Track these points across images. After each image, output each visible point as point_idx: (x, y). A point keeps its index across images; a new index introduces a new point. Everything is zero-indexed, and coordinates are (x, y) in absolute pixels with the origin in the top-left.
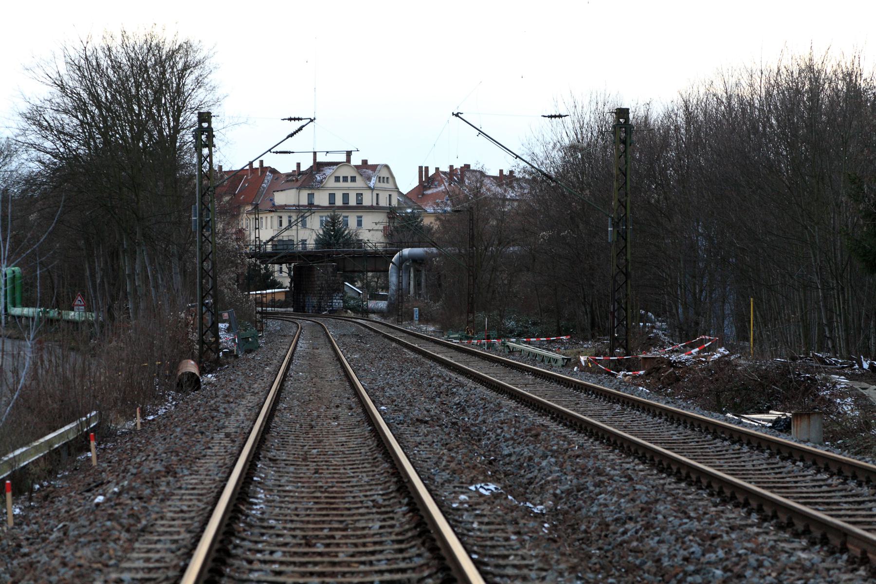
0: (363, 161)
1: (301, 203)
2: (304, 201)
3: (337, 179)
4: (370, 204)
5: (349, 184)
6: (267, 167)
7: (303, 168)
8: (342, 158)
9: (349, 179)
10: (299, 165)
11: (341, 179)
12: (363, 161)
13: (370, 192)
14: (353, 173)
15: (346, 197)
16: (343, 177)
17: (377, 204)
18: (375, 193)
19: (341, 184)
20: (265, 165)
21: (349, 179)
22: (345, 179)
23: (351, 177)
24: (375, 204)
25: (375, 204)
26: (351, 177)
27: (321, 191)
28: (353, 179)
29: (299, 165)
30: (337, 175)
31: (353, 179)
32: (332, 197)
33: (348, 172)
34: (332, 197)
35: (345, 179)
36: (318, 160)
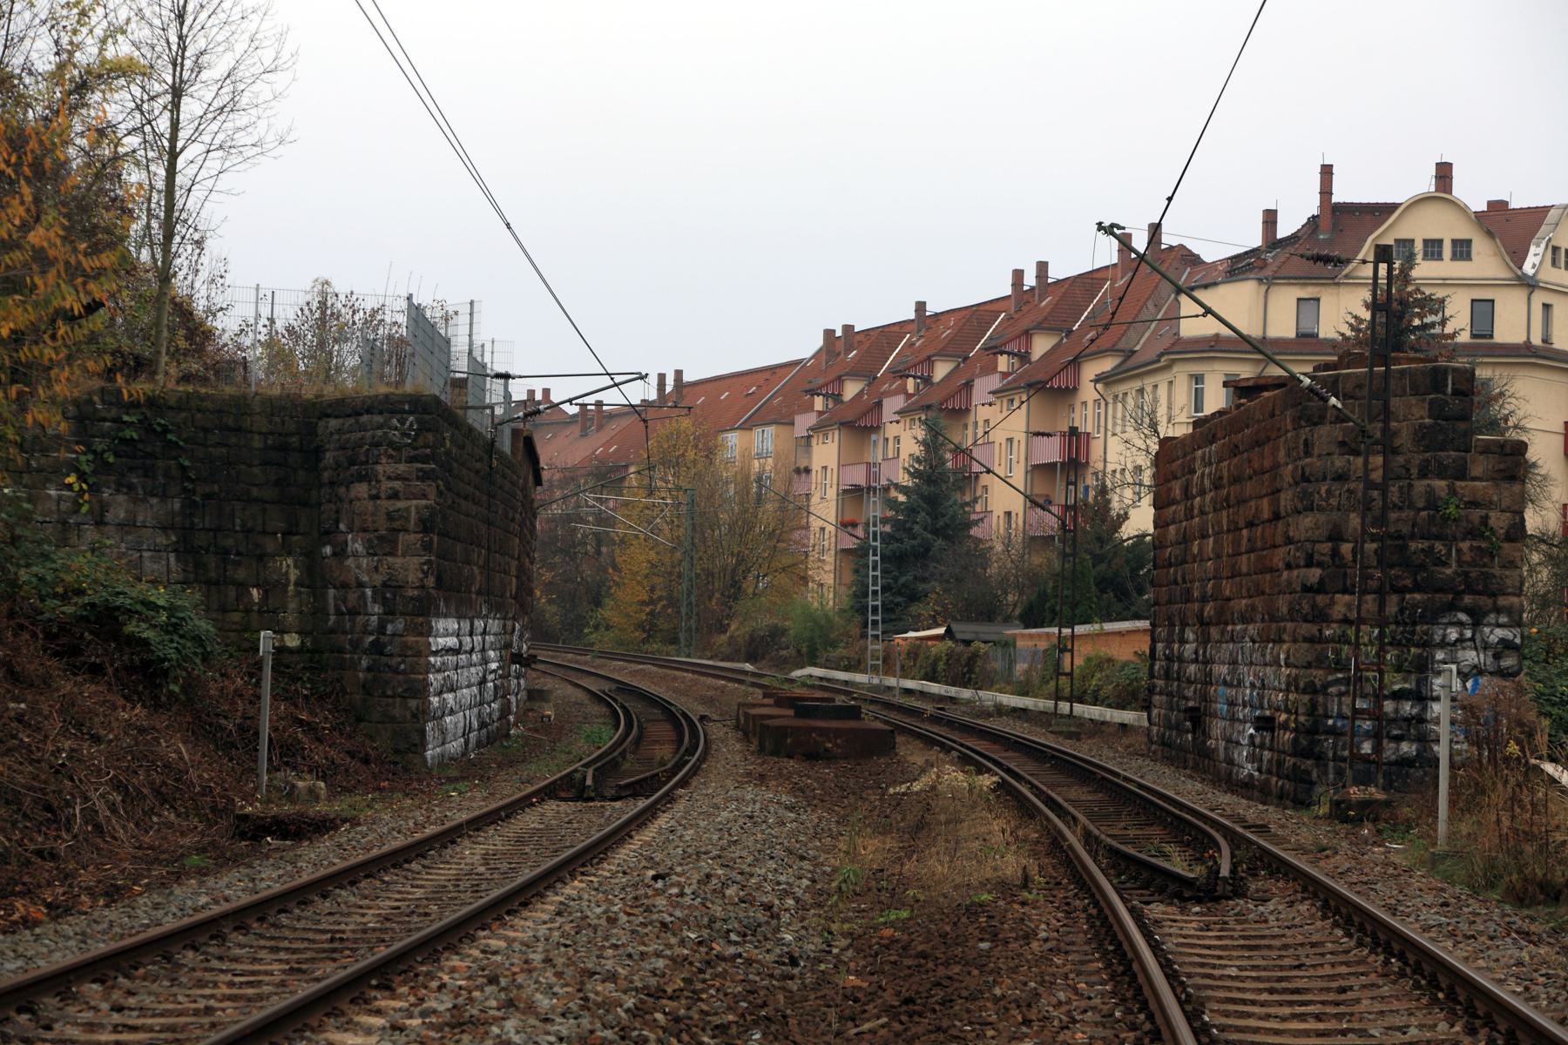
0: (1490, 204)
1: (1273, 333)
4: (1518, 338)
5: (1447, 267)
6: (1171, 248)
7: (1283, 231)
10: (1270, 218)
12: (1490, 204)
13: (1519, 296)
14: (1463, 231)
17: (1544, 341)
18: (1539, 298)
23: (1455, 242)
24: (1536, 340)
25: (1536, 340)
26: (1455, 242)
27: (1342, 290)
28: (1462, 250)
29: (1270, 218)
33: (1445, 227)
36: (1338, 197)
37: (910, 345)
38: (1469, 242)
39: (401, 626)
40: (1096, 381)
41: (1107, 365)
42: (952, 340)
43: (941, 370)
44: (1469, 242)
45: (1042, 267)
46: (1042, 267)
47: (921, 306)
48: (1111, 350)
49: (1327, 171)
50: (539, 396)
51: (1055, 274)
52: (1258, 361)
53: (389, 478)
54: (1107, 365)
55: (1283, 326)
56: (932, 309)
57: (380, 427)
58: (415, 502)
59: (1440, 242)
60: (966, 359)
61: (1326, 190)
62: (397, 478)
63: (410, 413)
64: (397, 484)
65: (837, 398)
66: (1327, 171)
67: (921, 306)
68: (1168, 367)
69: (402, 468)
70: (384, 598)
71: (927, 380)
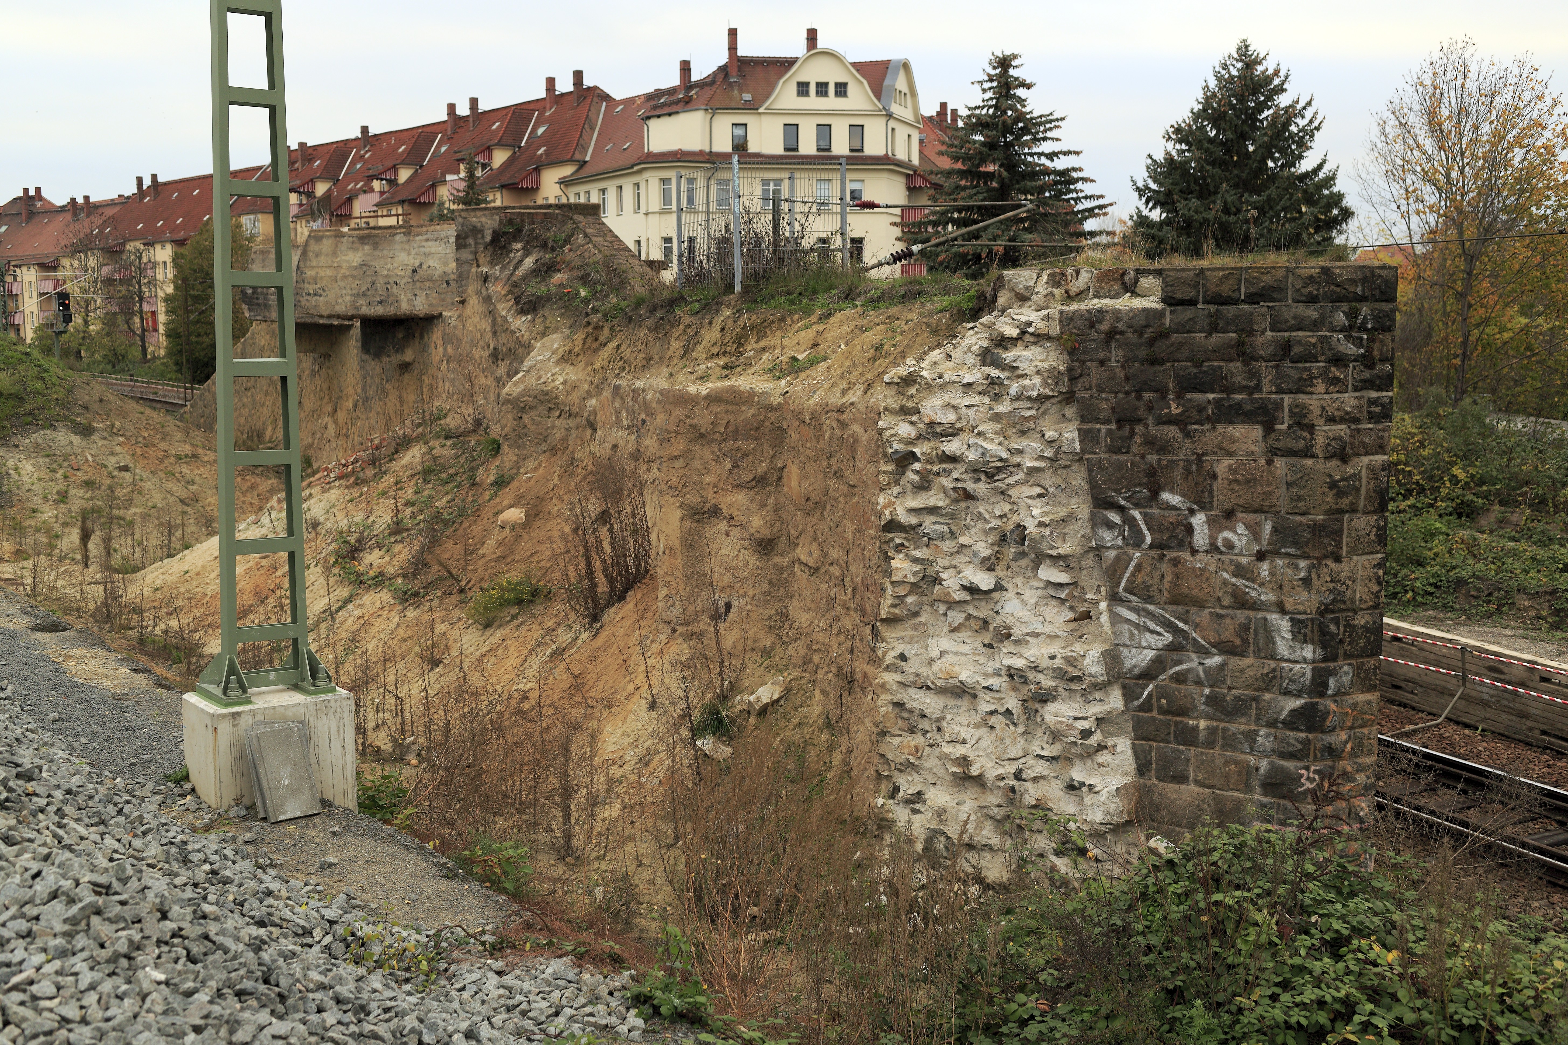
1: (715, 149)
2: (723, 144)
3: (803, 89)
5: (832, 102)
6: (589, 88)
8: (796, 48)
9: (831, 89)
10: (685, 67)
11: (813, 89)
15: (824, 131)
16: (818, 84)
19: (813, 102)
20: (588, 82)
21: (831, 89)
22: (822, 89)
27: (763, 117)
28: (841, 89)
29: (685, 67)
30: (803, 79)
31: (841, 89)
32: (791, 131)
34: (791, 131)
35: (822, 89)
37: (359, 158)
38: (845, 85)
39: (1346, 679)
40: (560, 183)
41: (567, 171)
42: (409, 152)
43: (404, 175)
44: (845, 85)
45: (474, 102)
46: (474, 102)
47: (365, 130)
48: (571, 161)
49: (733, 33)
50: (32, 193)
51: (483, 107)
52: (708, 169)
53: (1331, 420)
54: (567, 171)
55: (723, 144)
56: (372, 131)
57: (1315, 325)
58: (1366, 460)
59: (826, 85)
60: (421, 166)
61: (733, 47)
62: (1342, 420)
63: (1362, 299)
64: (1341, 430)
65: (310, 194)
66: (733, 33)
67: (365, 130)
68: (640, 172)
69: (1349, 400)
70: (1323, 632)
71: (392, 182)
